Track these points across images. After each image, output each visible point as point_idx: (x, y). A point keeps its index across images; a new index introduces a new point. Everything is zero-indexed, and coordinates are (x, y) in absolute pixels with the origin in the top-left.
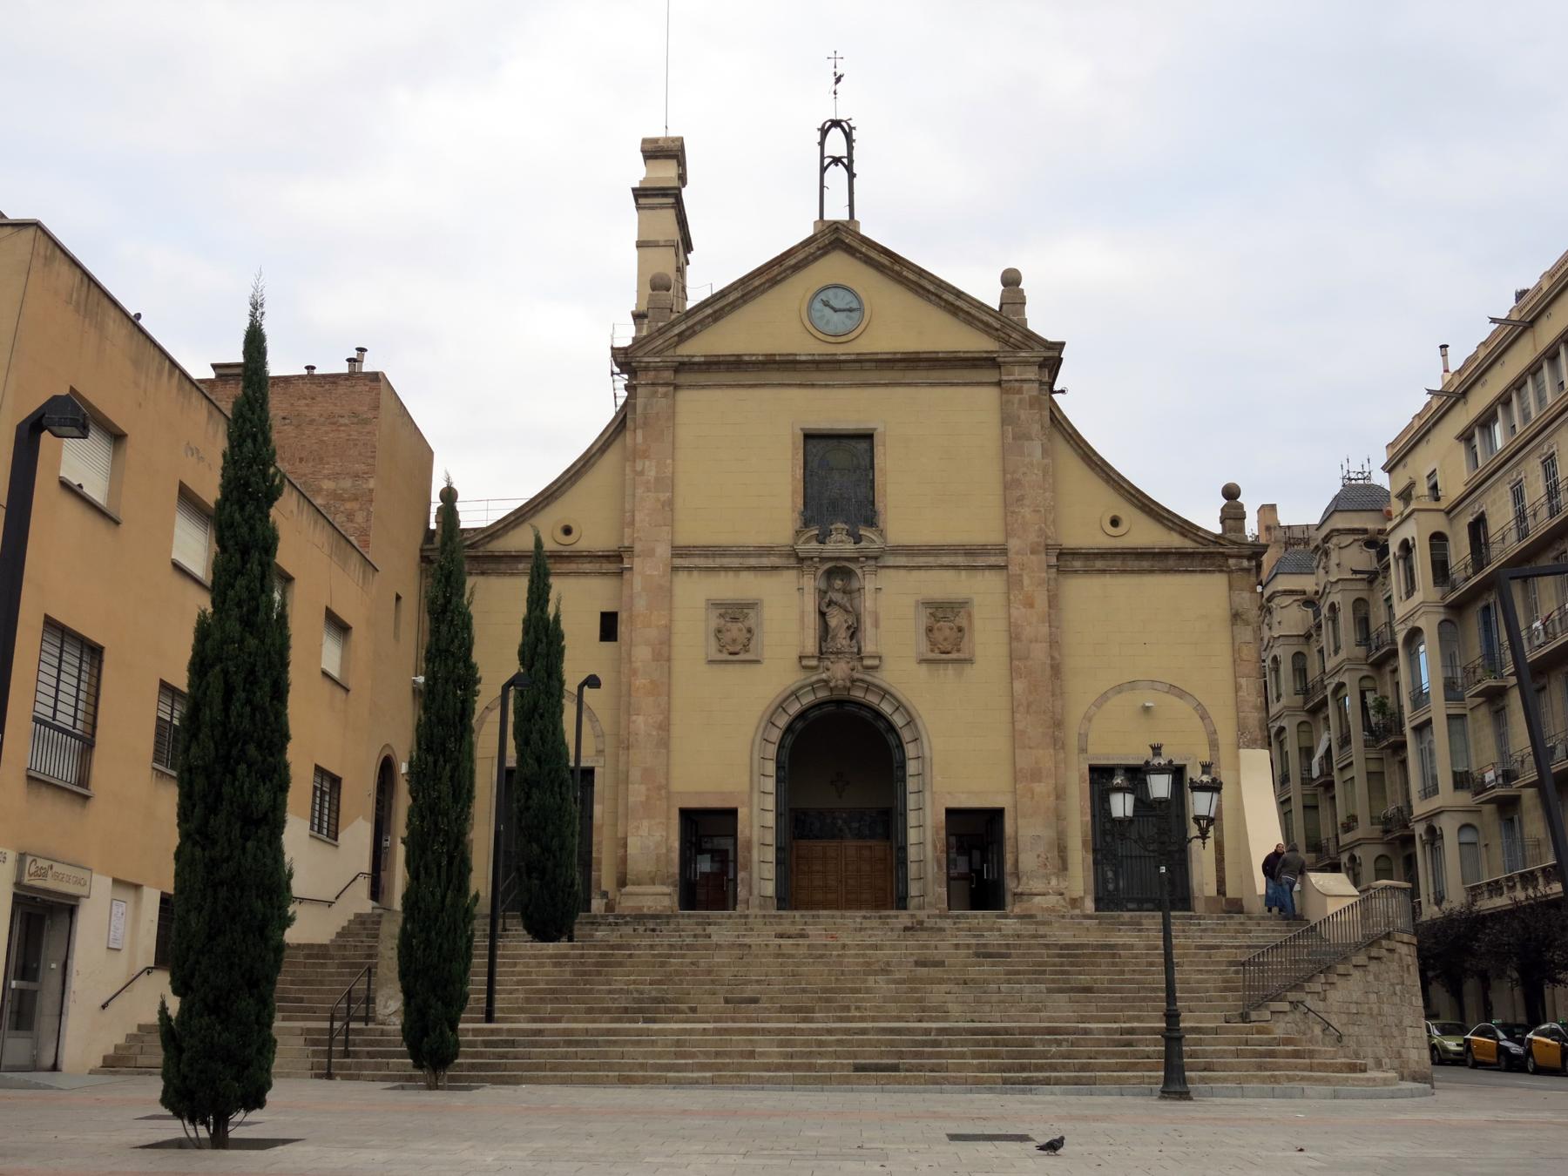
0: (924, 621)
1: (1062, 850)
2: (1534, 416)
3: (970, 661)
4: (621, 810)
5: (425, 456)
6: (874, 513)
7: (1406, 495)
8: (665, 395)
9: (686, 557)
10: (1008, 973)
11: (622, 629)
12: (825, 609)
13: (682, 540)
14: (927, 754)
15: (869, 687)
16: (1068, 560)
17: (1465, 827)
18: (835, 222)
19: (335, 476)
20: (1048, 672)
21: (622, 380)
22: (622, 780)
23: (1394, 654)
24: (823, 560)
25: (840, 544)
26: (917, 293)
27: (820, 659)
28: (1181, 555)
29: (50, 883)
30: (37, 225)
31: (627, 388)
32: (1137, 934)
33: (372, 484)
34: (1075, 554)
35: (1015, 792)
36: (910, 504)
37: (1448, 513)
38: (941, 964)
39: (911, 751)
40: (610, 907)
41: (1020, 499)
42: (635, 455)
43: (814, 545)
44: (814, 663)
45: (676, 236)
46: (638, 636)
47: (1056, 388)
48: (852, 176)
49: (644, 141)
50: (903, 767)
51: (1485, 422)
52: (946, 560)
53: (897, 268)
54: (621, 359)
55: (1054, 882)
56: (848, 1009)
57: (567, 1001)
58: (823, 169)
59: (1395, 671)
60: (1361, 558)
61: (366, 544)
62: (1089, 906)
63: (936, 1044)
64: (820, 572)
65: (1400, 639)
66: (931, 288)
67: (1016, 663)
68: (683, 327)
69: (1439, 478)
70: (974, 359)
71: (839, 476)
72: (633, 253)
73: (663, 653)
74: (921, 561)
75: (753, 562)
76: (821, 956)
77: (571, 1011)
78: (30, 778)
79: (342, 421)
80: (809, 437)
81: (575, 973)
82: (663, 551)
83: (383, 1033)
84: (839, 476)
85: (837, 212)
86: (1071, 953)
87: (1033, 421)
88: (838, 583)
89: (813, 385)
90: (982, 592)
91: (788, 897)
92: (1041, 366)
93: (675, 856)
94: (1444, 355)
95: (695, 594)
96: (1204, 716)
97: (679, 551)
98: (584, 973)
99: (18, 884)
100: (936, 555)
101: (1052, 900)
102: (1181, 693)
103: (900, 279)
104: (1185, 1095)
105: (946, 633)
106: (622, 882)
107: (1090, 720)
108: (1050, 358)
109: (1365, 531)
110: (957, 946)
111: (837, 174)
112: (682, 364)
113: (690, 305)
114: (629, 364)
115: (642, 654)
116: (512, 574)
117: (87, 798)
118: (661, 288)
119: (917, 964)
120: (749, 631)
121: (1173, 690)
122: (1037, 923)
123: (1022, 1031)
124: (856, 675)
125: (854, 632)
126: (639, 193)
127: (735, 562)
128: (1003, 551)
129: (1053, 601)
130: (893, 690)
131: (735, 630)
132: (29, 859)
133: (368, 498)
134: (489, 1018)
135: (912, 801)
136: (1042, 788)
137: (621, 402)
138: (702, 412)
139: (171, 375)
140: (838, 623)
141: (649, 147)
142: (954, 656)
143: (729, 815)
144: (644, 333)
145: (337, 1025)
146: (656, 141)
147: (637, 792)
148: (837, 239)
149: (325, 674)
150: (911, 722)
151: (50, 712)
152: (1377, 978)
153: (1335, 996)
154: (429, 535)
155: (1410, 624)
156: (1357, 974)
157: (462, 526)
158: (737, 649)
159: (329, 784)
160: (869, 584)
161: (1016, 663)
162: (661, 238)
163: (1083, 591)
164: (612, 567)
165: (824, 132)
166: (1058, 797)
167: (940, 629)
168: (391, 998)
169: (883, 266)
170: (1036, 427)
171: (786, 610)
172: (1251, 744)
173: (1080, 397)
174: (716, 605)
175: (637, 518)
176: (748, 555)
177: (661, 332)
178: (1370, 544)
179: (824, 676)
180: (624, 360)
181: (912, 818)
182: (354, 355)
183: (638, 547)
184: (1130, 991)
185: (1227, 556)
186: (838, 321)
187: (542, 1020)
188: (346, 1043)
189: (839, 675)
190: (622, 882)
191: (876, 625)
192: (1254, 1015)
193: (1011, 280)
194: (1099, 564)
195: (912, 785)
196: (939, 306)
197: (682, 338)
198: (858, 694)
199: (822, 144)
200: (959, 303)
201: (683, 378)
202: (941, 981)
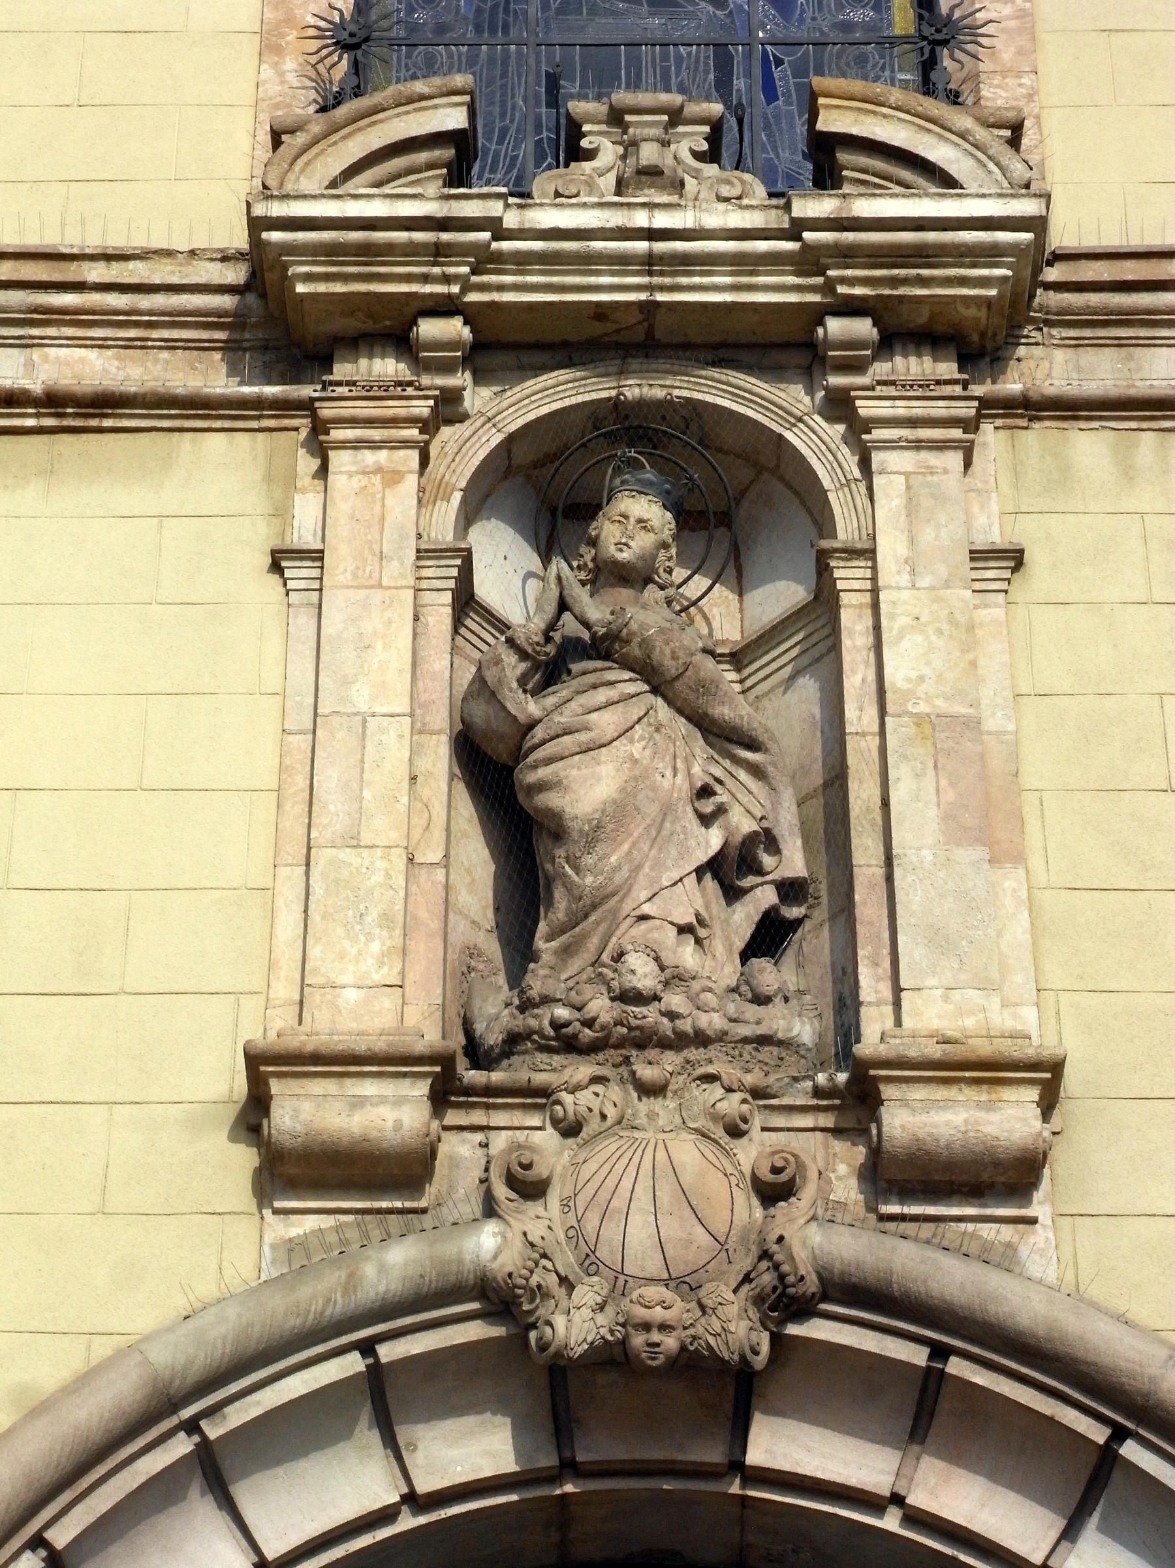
27: (445, 1094)
44: (390, 1112)
160: (910, 506)
179: (488, 1245)
189: (641, 1236)
191: (991, 824)
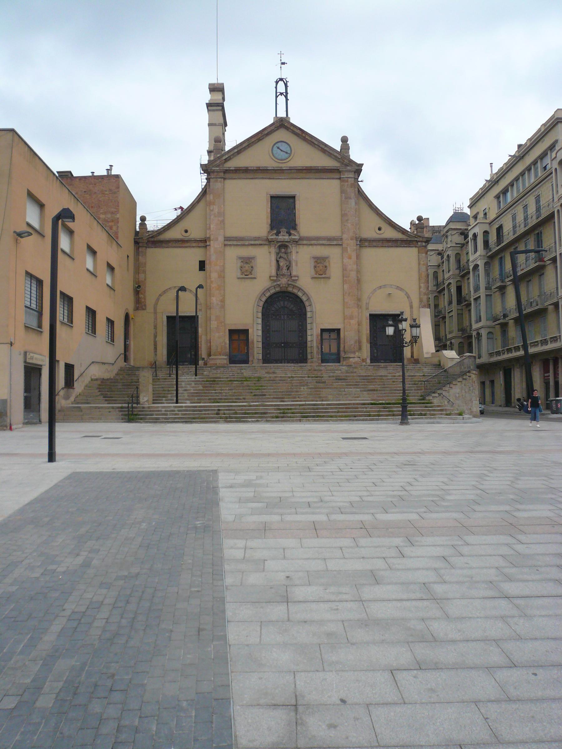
0: (313, 264)
1: (360, 342)
2: (521, 191)
3: (329, 278)
4: (208, 330)
5: (133, 204)
6: (296, 225)
7: (475, 217)
8: (220, 182)
9: (230, 241)
10: (347, 385)
11: (207, 267)
12: (278, 259)
13: (228, 234)
14: (314, 310)
15: (294, 287)
16: (363, 243)
17: (489, 333)
18: (282, 118)
19: (105, 213)
20: (356, 281)
21: (205, 176)
22: (208, 320)
23: (468, 273)
24: (278, 242)
25: (283, 237)
26: (311, 144)
28: (402, 241)
29: (34, 361)
30: (13, 131)
31: (206, 179)
32: (390, 371)
33: (118, 216)
34: (366, 240)
35: (344, 323)
36: (308, 222)
37: (490, 224)
38: (324, 382)
39: (308, 309)
40: (205, 364)
41: (347, 220)
42: (210, 204)
43: (274, 237)
44: (275, 278)
45: (222, 121)
46: (212, 269)
47: (359, 180)
48: (287, 100)
49: (210, 84)
50: (306, 314)
51: (505, 192)
52: (321, 242)
53: (304, 135)
54: (205, 168)
55: (357, 354)
56: (295, 398)
57: (202, 396)
58: (277, 97)
59: (468, 279)
60: (459, 239)
61: (117, 238)
62: (368, 361)
63: (326, 408)
64: (277, 246)
65: (471, 268)
66: (316, 143)
67: (345, 278)
68: (227, 156)
69: (487, 211)
70: (331, 169)
71: (283, 212)
72: (207, 128)
73: (222, 276)
74: (313, 242)
75: (253, 242)
76: (284, 380)
77: (203, 400)
78: (25, 326)
79: (106, 193)
80: (272, 197)
81: (203, 387)
82: (221, 239)
83: (143, 408)
84: (283, 212)
85: (282, 114)
86: (368, 379)
87: (352, 192)
88: (283, 250)
89: (273, 179)
90: (333, 253)
91: (267, 359)
92: (355, 172)
93: (228, 346)
94: (491, 167)
95: (233, 254)
96: (408, 297)
97: (227, 239)
98: (206, 387)
99: (25, 362)
100: (317, 240)
101: (356, 359)
102: (401, 290)
103: (305, 139)
104: (407, 423)
105: (321, 267)
106: (209, 355)
107: (370, 298)
108: (358, 169)
109: (460, 229)
110: (330, 377)
111: (281, 99)
112: (226, 170)
113: (227, 148)
114: (207, 170)
115: (214, 275)
116: (167, 247)
117: (42, 332)
118: (217, 142)
119: (317, 382)
120: (252, 267)
121: (398, 288)
122: (353, 368)
123: (354, 404)
124: (290, 283)
125: (289, 268)
126: (209, 105)
127: (247, 243)
128: (341, 239)
129: (358, 257)
130: (302, 288)
131: (247, 267)
132: (28, 354)
133: (117, 221)
134: (177, 402)
135: (309, 327)
136: (353, 322)
137: (205, 184)
138: (235, 188)
139: (57, 181)
140: (283, 266)
141: (212, 87)
142: (323, 276)
143: (246, 332)
144: (212, 158)
145: (130, 405)
146: (214, 84)
147: (214, 324)
148: (282, 124)
149: (108, 285)
150: (309, 299)
151: (29, 304)
152: (465, 385)
153: (452, 391)
154: (137, 233)
155: (475, 263)
156: (459, 384)
157: (149, 229)
158: (248, 274)
159: (111, 323)
161: (345, 278)
162: (217, 122)
163: (369, 253)
164: (202, 244)
165: (277, 82)
166: (359, 325)
167: (319, 267)
168: (145, 396)
169: (299, 134)
170: (353, 195)
171: (265, 260)
172: (424, 307)
173: (369, 183)
174: (241, 258)
175: (212, 226)
176: (251, 240)
177: (219, 158)
178: (462, 234)
179: (278, 283)
180: (205, 169)
181: (309, 332)
182: (109, 168)
183: (212, 238)
184: (387, 390)
185: (417, 242)
186: (284, 155)
187: (194, 403)
188: (132, 411)
189: (284, 283)
190: (209, 355)
191: (297, 265)
192: (427, 398)
193: (344, 140)
194: (374, 244)
195: (309, 321)
196: (319, 150)
197: (226, 160)
198: (290, 289)
199: (276, 88)
200: (326, 148)
201: (227, 175)
202: (325, 388)
